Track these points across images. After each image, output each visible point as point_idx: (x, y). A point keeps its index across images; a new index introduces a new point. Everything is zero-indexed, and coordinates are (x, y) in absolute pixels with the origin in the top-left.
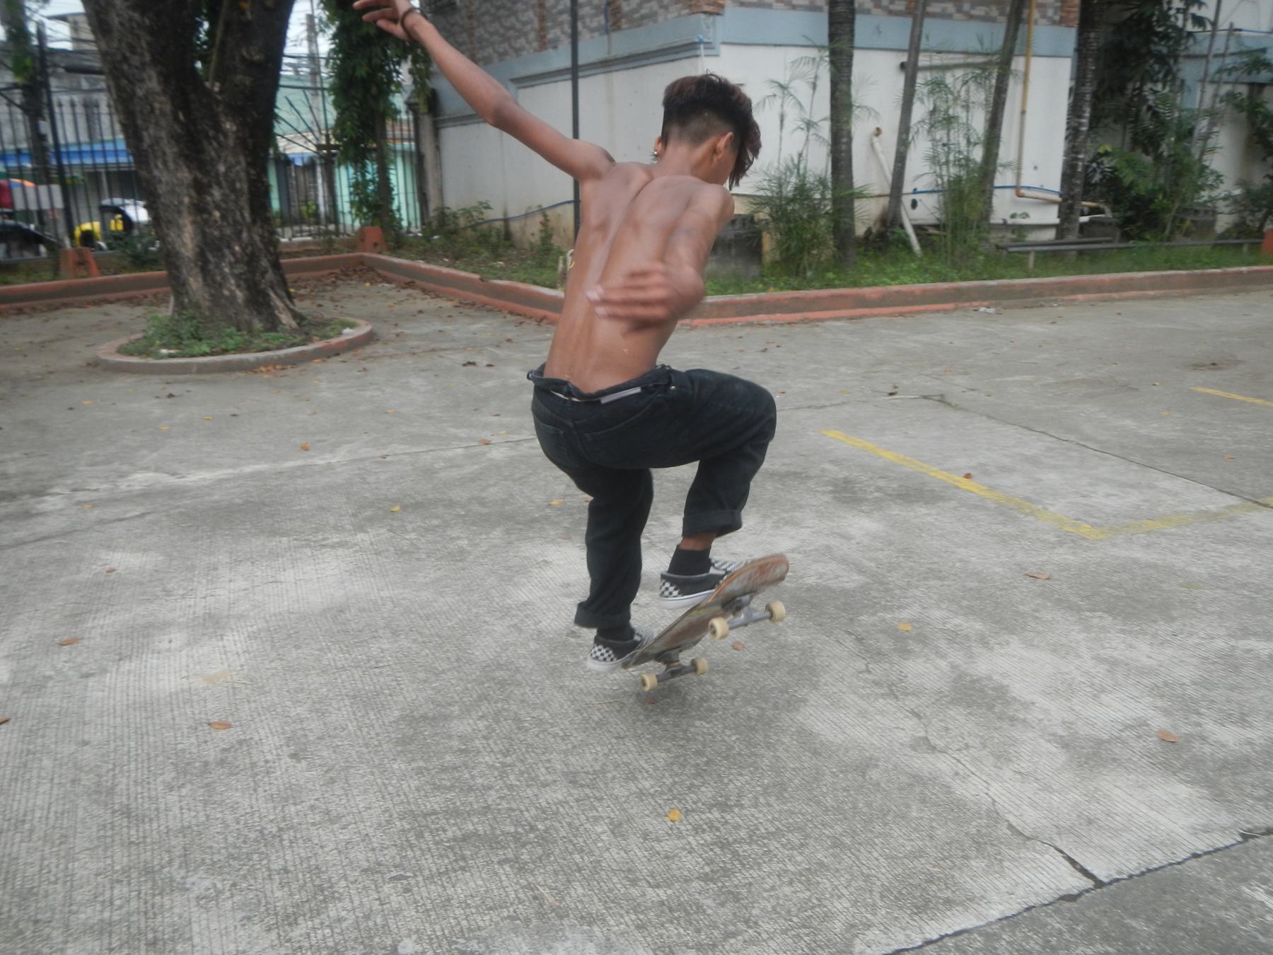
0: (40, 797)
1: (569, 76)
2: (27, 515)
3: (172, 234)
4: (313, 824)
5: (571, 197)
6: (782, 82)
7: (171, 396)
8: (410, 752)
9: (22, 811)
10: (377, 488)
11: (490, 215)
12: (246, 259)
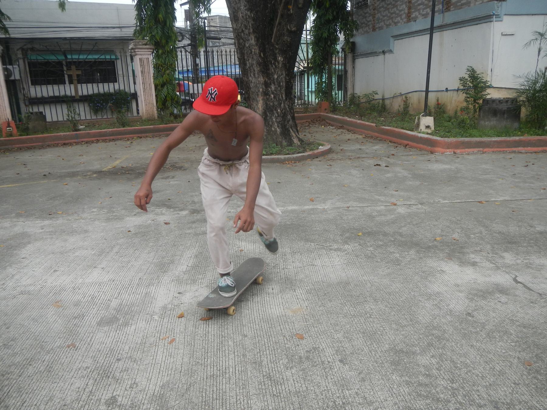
0: (230, 361)
1: (429, 32)
4: (359, 403)
5: (425, 90)
6: (541, 32)
8: (400, 370)
9: (224, 369)
10: (349, 223)
11: (376, 97)
12: (282, 115)
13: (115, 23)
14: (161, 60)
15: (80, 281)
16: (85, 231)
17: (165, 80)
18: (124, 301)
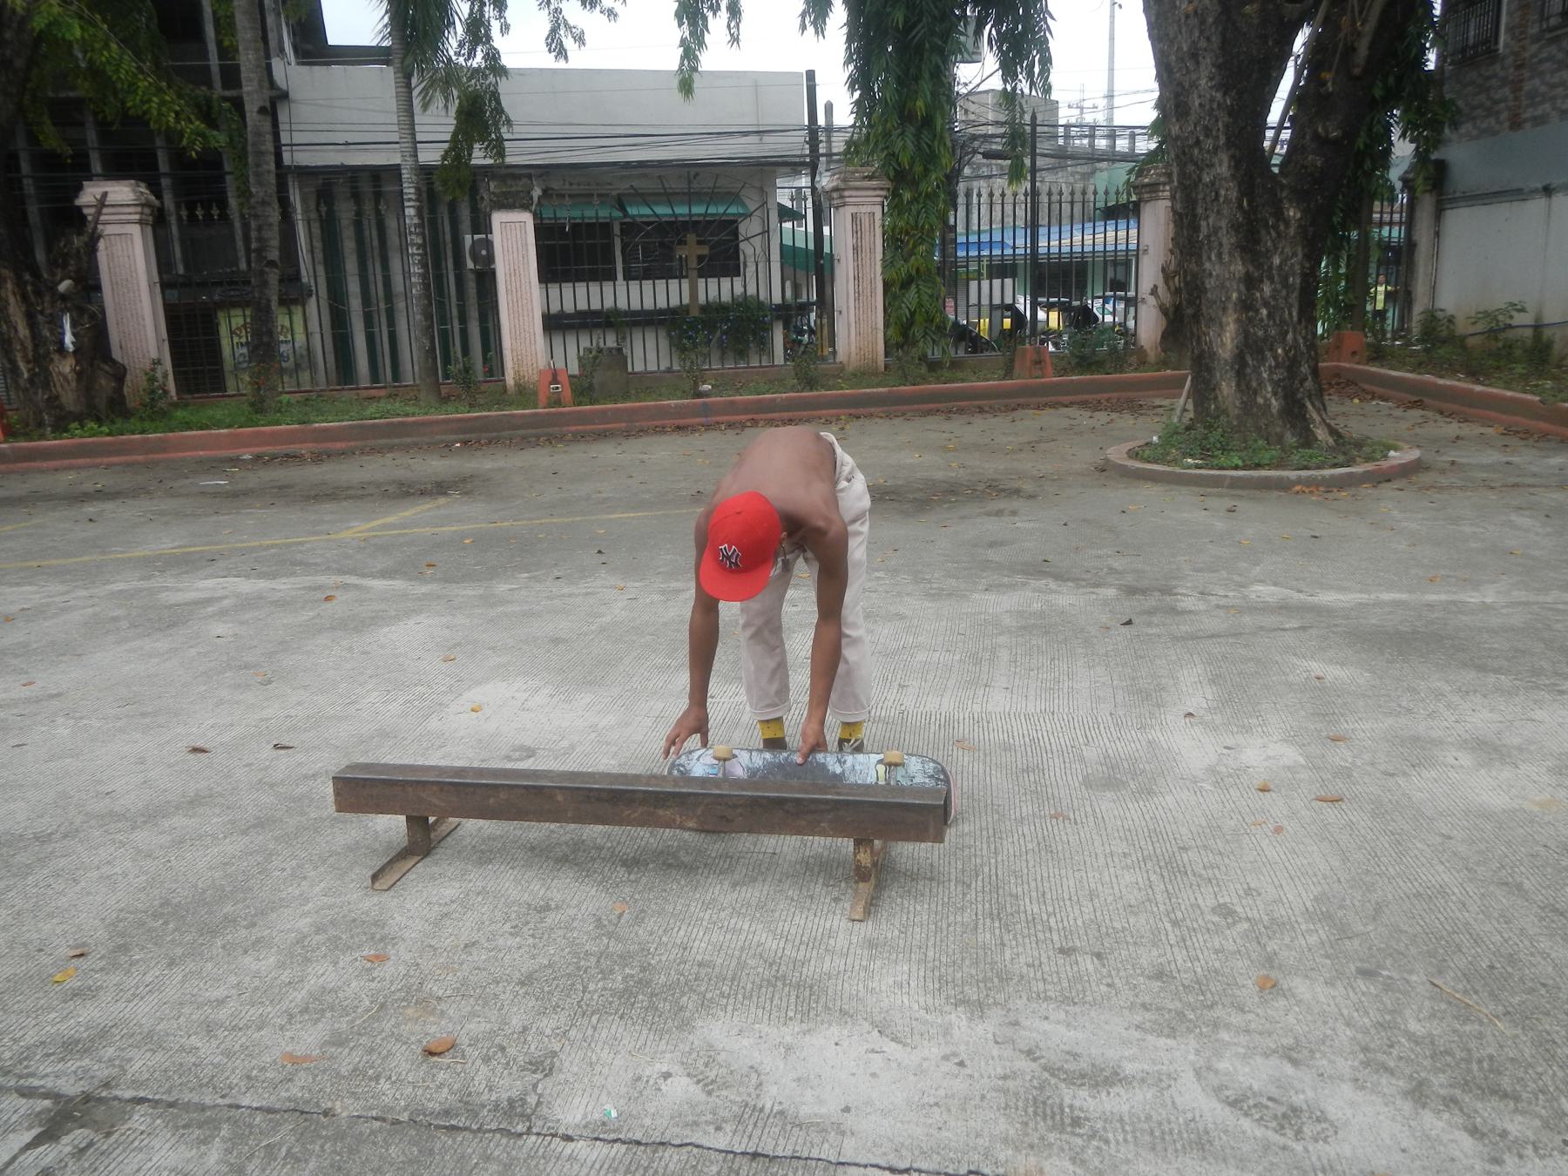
2: (1174, 611)
11: (1519, 319)
12: (1287, 363)
13: (748, 121)
15: (977, 708)
18: (1110, 751)
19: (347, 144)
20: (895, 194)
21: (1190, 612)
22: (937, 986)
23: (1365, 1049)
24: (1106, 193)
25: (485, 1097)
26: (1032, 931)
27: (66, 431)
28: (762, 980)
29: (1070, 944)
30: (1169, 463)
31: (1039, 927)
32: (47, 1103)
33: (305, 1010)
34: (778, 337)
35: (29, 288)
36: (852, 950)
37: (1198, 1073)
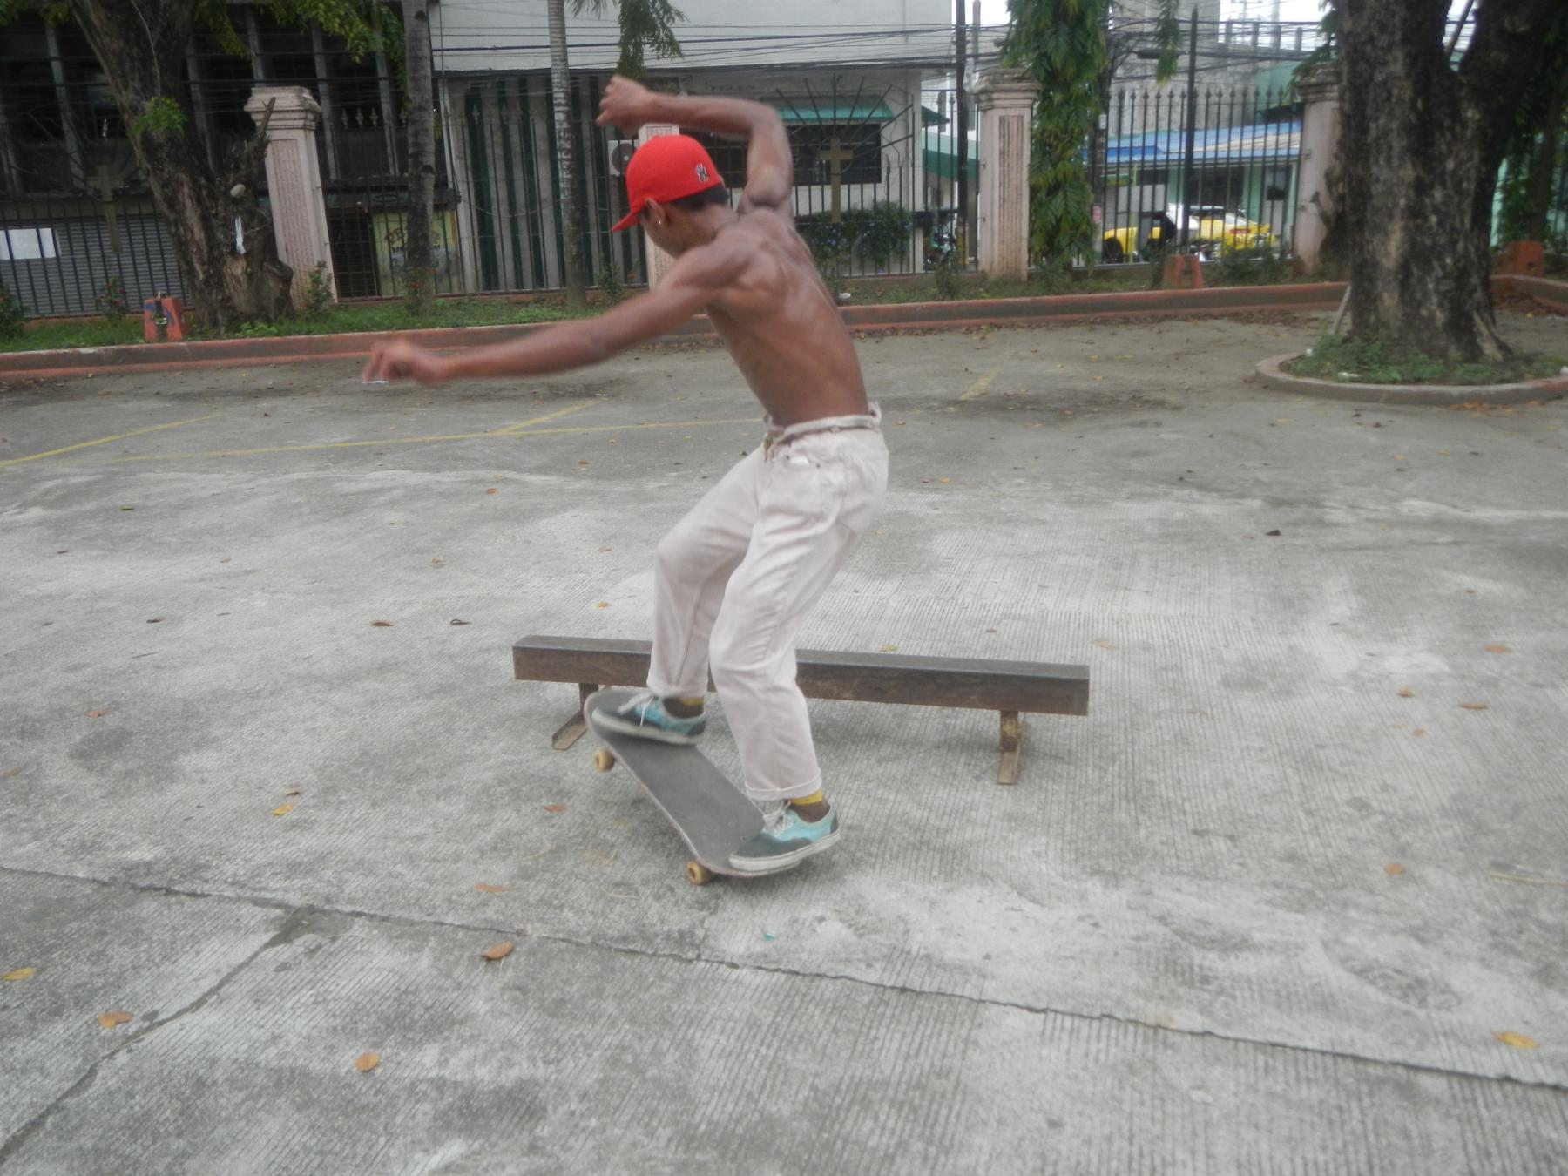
2: (1320, 523)
3: (1375, 242)
7: (1377, 425)
12: (1456, 273)
13: (893, 21)
14: (1056, 119)
15: (1116, 610)
16: (1037, 520)
17: (1060, 177)
19: (495, 48)
20: (1045, 97)
21: (1337, 525)
22: (1074, 857)
23: (1494, 933)
24: (1269, 94)
25: (658, 928)
26: (1167, 813)
27: (238, 331)
28: (908, 843)
29: (1204, 827)
30: (1322, 376)
31: (1174, 810)
32: (279, 912)
33: (494, 848)
34: (918, 244)
35: (204, 192)
36: (993, 822)
37: (1325, 945)
